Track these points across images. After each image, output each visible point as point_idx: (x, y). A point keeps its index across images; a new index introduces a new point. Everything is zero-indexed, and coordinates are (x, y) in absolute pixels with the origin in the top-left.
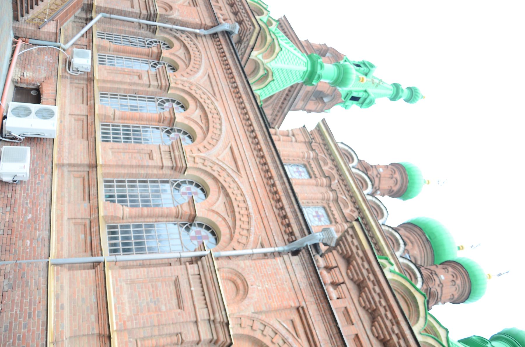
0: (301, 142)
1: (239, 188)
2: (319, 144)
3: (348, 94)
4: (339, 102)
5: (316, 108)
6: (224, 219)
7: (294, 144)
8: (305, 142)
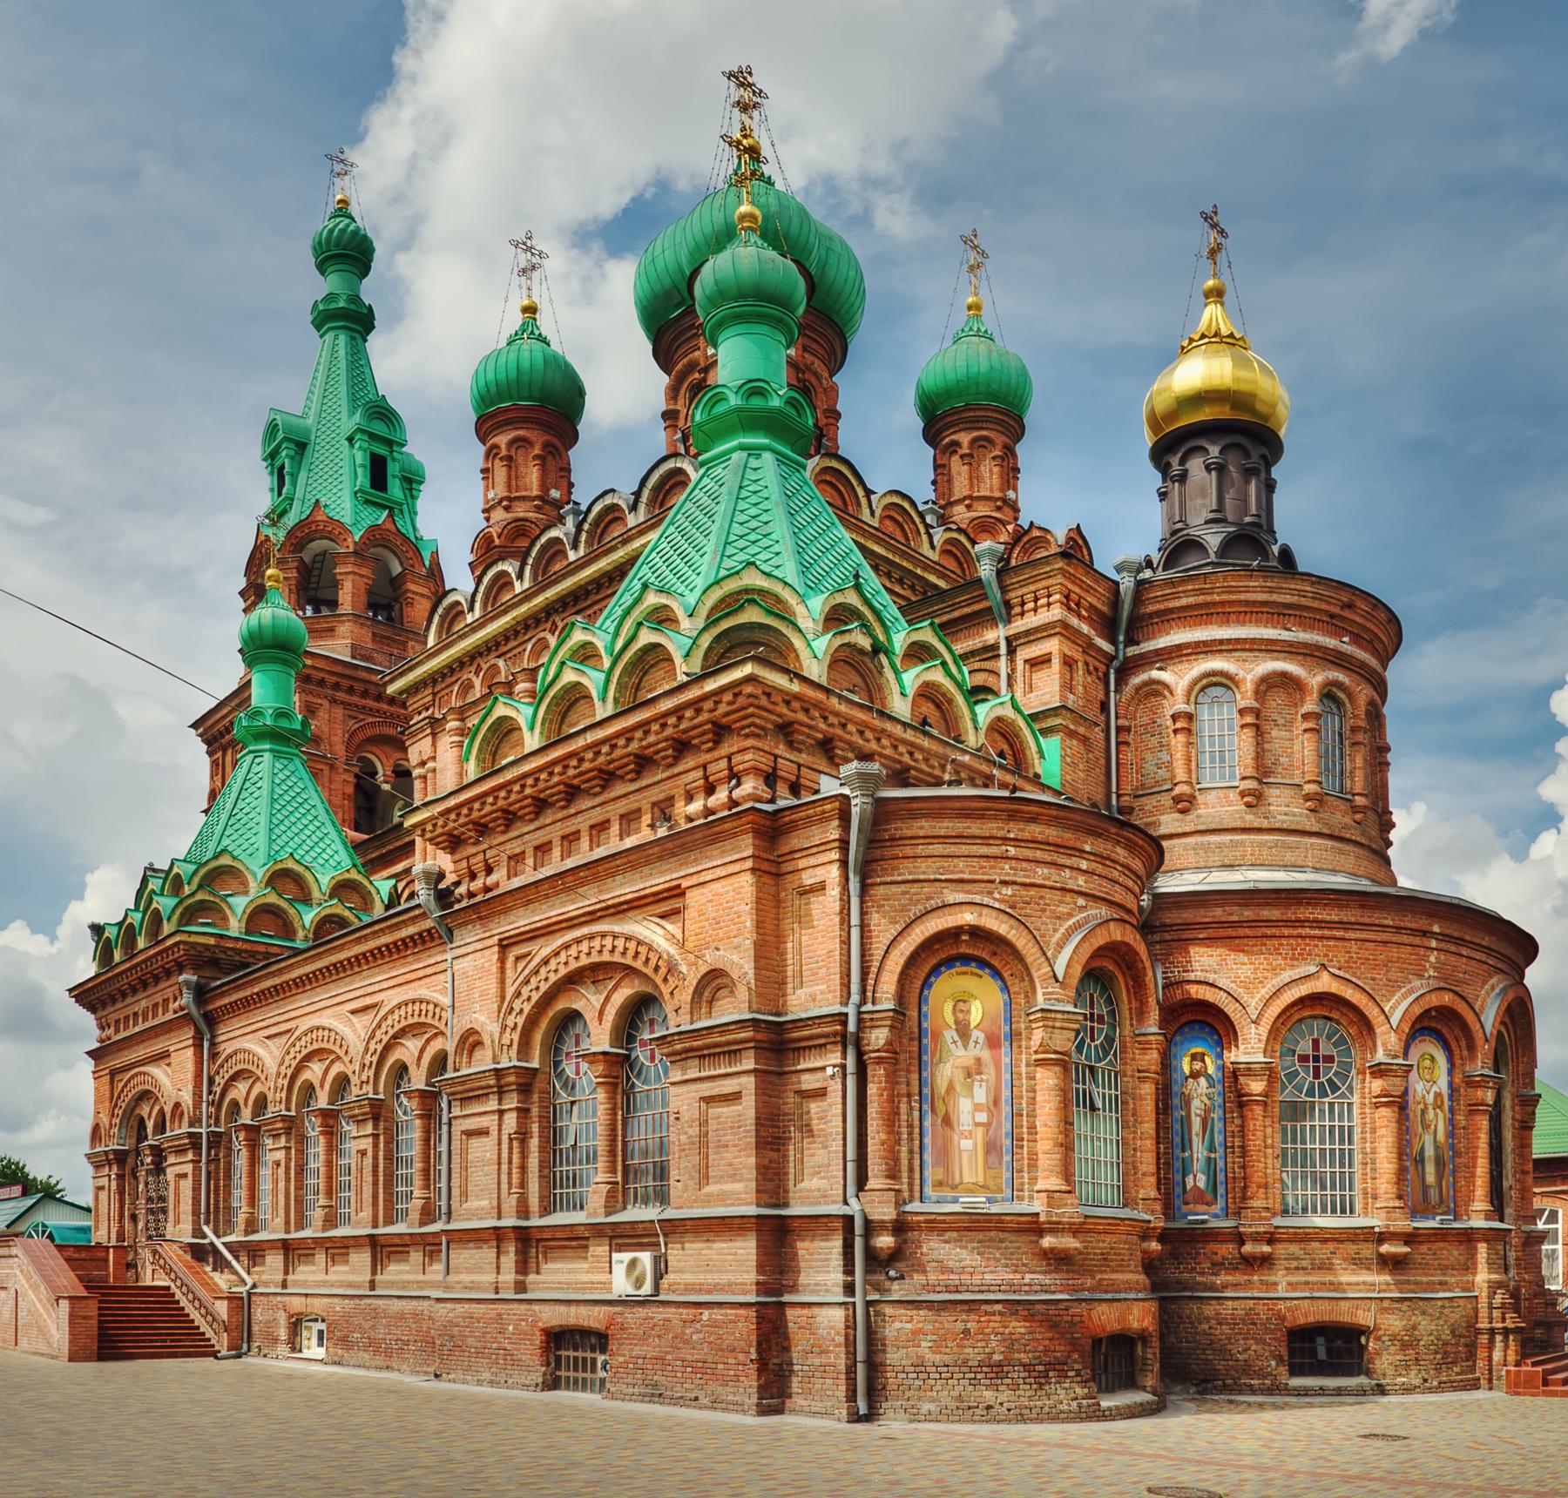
0: (434, 744)
1: (392, 1012)
2: (434, 694)
3: (367, 502)
4: (393, 529)
5: (422, 595)
6: (428, 1041)
7: (438, 765)
8: (434, 735)
